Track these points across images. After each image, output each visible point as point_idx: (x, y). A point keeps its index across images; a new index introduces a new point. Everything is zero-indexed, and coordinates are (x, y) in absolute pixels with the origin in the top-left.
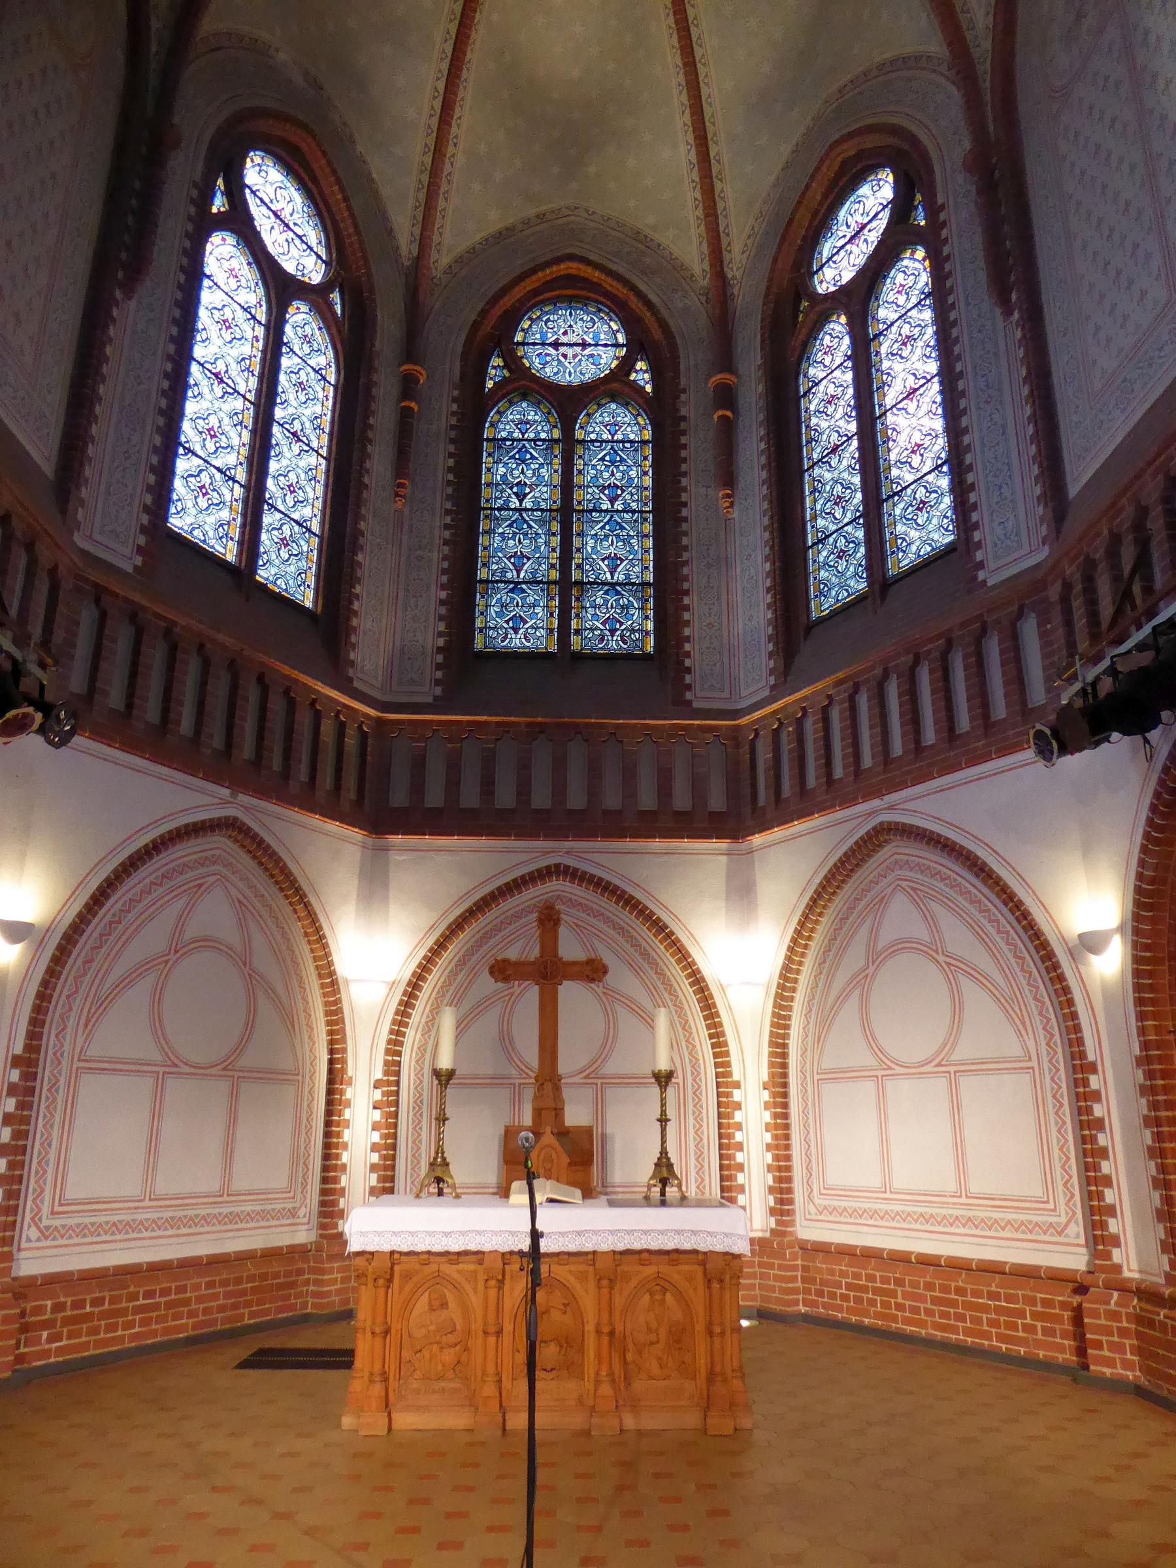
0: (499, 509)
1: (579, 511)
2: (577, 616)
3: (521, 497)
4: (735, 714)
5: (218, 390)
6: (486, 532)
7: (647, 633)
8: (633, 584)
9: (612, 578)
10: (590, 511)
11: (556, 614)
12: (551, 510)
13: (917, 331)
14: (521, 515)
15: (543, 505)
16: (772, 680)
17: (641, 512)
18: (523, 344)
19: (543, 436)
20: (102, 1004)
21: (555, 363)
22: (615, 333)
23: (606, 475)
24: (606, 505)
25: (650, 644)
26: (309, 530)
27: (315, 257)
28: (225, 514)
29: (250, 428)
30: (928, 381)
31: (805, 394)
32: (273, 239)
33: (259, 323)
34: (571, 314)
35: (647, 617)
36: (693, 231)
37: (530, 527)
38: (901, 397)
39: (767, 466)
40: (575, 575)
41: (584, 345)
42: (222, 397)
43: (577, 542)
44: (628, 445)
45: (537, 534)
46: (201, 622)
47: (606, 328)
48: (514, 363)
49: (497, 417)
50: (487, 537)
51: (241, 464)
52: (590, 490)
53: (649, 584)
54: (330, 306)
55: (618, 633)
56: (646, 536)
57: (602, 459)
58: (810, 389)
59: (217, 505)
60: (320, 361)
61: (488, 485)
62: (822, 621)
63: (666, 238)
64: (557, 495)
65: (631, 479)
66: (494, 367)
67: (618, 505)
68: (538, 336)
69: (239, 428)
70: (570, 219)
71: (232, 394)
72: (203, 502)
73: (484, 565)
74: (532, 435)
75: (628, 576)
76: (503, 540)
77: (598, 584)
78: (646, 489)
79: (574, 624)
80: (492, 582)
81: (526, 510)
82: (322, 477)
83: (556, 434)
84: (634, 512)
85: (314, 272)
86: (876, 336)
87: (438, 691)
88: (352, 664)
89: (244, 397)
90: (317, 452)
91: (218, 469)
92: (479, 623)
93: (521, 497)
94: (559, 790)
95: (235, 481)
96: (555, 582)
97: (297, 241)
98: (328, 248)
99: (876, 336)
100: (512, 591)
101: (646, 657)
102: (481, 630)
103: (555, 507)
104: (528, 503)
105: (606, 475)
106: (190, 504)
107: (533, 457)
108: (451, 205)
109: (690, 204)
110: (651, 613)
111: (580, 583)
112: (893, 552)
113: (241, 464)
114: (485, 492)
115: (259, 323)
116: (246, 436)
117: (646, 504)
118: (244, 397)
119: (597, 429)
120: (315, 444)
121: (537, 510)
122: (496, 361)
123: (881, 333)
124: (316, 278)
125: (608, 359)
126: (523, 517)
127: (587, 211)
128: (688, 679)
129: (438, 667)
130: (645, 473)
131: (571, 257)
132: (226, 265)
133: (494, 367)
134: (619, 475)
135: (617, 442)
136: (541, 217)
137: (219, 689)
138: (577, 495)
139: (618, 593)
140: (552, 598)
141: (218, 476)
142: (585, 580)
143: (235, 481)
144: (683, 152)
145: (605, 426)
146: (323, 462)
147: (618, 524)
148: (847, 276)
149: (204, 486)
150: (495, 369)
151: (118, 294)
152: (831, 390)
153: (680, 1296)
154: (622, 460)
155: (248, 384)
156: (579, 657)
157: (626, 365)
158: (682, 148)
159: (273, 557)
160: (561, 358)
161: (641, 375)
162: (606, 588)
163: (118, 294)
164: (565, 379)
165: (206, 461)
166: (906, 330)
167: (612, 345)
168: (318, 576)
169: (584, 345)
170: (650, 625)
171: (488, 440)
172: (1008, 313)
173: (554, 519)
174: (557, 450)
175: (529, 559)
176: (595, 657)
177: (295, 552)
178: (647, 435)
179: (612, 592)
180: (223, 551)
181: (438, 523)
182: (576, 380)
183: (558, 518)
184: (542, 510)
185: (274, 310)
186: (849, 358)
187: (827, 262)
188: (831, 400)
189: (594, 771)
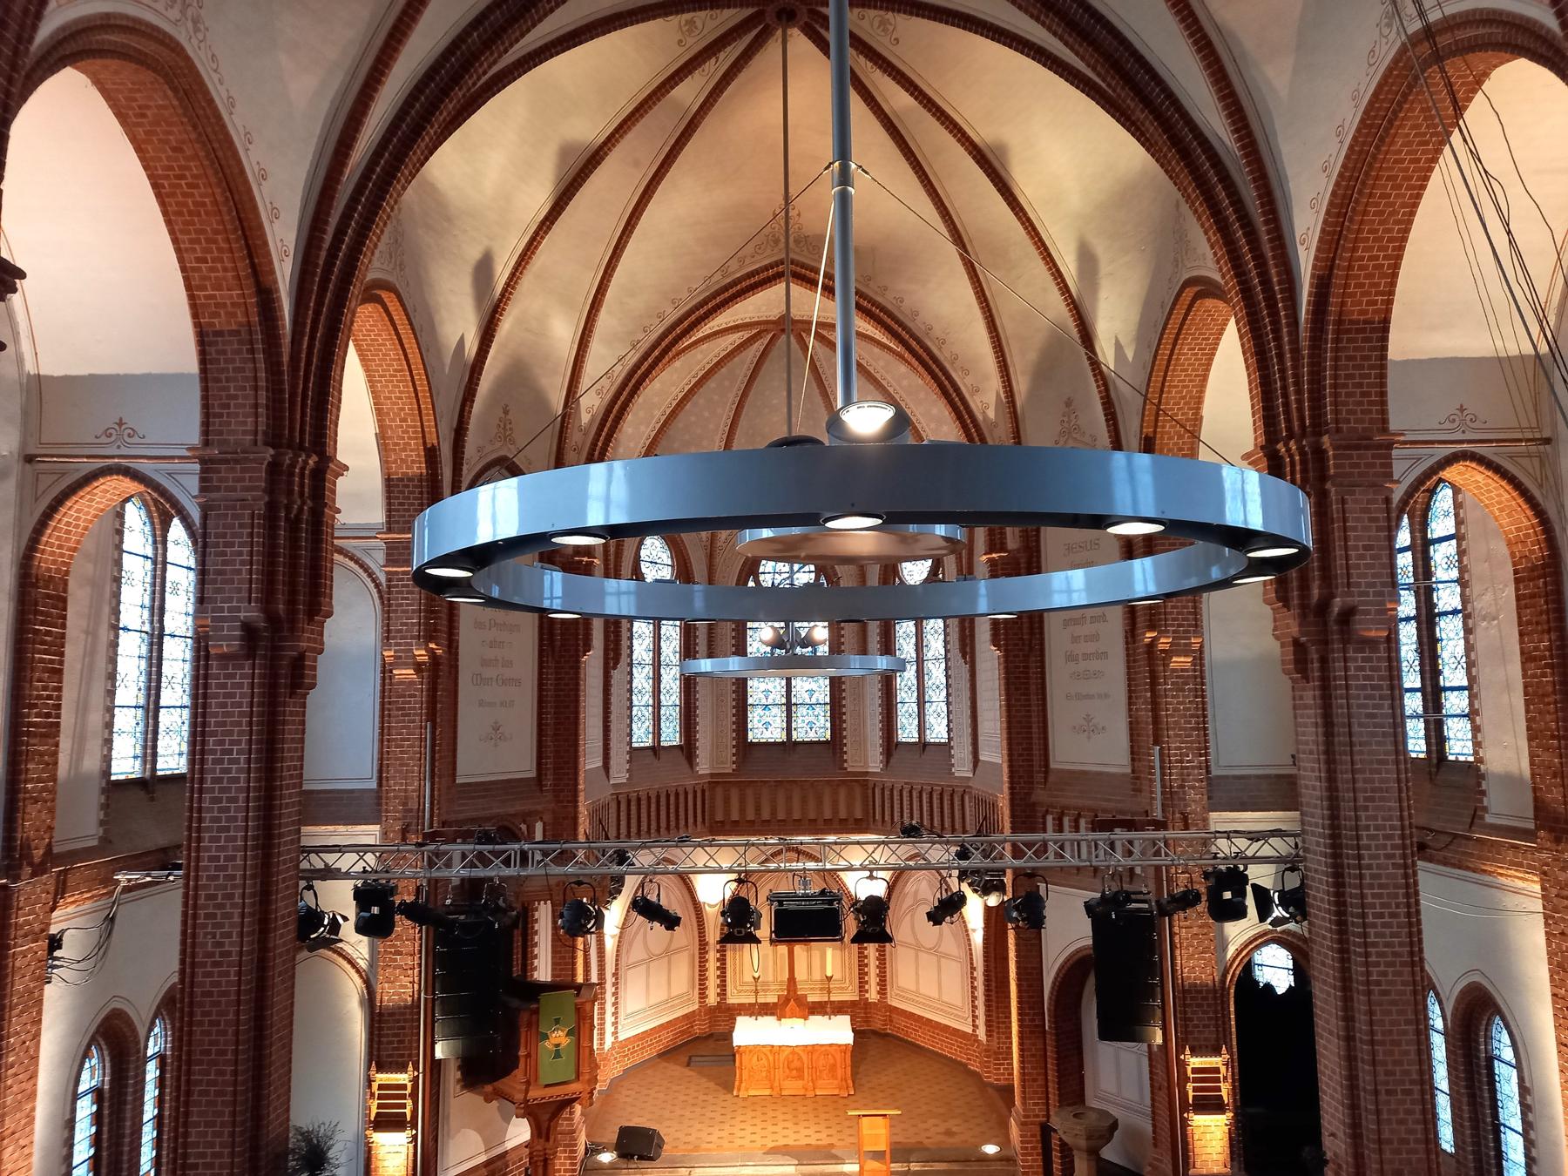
4: (867, 773)
20: (631, 945)
25: (828, 736)
28: (647, 723)
40: (794, 701)
79: (794, 725)
92: (750, 726)
94: (789, 811)
101: (827, 742)
137: (653, 807)
156: (796, 743)
170: (828, 725)
176: (804, 743)
189: (804, 801)
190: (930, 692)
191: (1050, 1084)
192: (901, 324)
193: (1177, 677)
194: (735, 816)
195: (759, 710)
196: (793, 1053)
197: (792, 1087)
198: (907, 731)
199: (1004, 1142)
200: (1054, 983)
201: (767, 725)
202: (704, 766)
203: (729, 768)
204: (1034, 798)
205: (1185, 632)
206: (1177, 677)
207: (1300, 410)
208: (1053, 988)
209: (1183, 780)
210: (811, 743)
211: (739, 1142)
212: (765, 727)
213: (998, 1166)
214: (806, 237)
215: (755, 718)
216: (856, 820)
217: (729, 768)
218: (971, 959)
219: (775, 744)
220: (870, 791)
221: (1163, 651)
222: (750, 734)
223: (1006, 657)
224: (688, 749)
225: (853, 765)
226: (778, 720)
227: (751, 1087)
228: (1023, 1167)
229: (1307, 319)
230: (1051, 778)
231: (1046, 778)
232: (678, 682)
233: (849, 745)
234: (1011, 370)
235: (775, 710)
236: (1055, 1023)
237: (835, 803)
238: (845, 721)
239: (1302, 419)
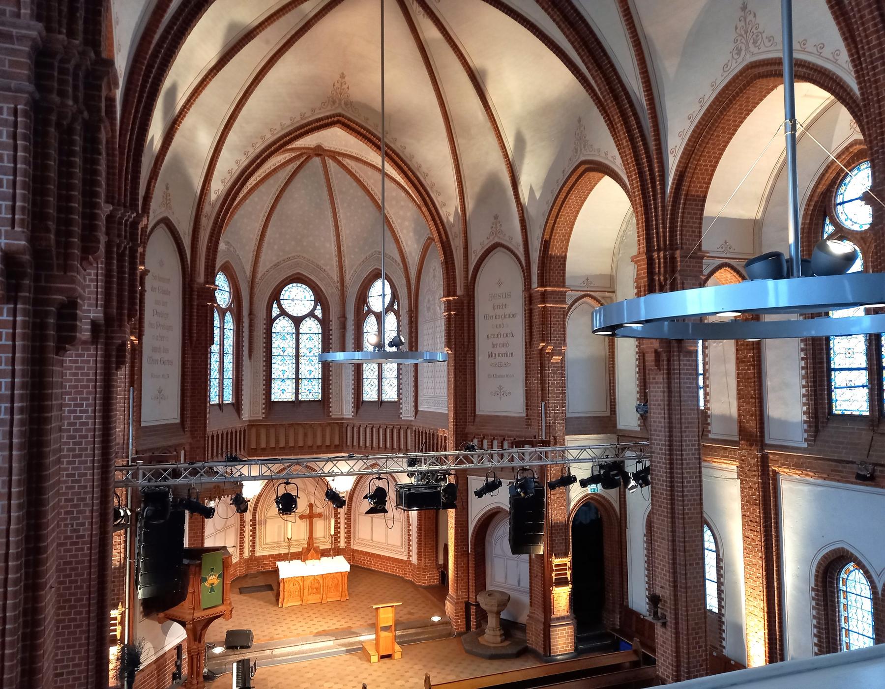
3: (284, 351)
24: (308, 354)
25: (320, 397)
40: (300, 377)
48: (280, 306)
63: (327, 268)
79: (300, 391)
83: (294, 331)
87: (264, 416)
93: (284, 351)
94: (296, 441)
101: (319, 401)
108: (263, 258)
109: (334, 260)
114: (273, 350)
122: (275, 305)
128: (331, 409)
129: (263, 409)
131: (298, 273)
144: (333, 247)
150: (275, 311)
153: (337, 579)
156: (301, 402)
157: (315, 308)
158: (333, 246)
161: (318, 313)
164: (295, 315)
170: (320, 391)
174: (294, 335)
176: (305, 401)
178: (320, 331)
182: (300, 315)
189: (305, 435)
190: (386, 372)
191: (470, 581)
192: (402, 160)
193: (554, 367)
194: (263, 445)
195: (279, 382)
196: (315, 579)
197: (313, 599)
198: (370, 394)
199: (443, 613)
200: (475, 528)
201: (283, 391)
202: (246, 416)
203: (260, 416)
204: (467, 430)
205: (559, 343)
206: (554, 367)
207: (664, 236)
208: (474, 530)
209: (555, 420)
210: (310, 401)
211: (296, 632)
212: (282, 392)
213: (441, 627)
214: (351, 103)
215: (276, 386)
216: (309, 447)
217: (260, 416)
218: (409, 520)
219: (288, 402)
220: (344, 429)
221: (548, 353)
222: (273, 396)
223: (455, 354)
224: (237, 405)
225: (334, 415)
226: (290, 388)
227: (289, 601)
228: (456, 626)
229: (671, 192)
230: (477, 420)
231: (474, 419)
232: (231, 364)
233: (333, 403)
234: (465, 195)
235: (288, 382)
236: (475, 549)
237: (323, 436)
239: (665, 241)
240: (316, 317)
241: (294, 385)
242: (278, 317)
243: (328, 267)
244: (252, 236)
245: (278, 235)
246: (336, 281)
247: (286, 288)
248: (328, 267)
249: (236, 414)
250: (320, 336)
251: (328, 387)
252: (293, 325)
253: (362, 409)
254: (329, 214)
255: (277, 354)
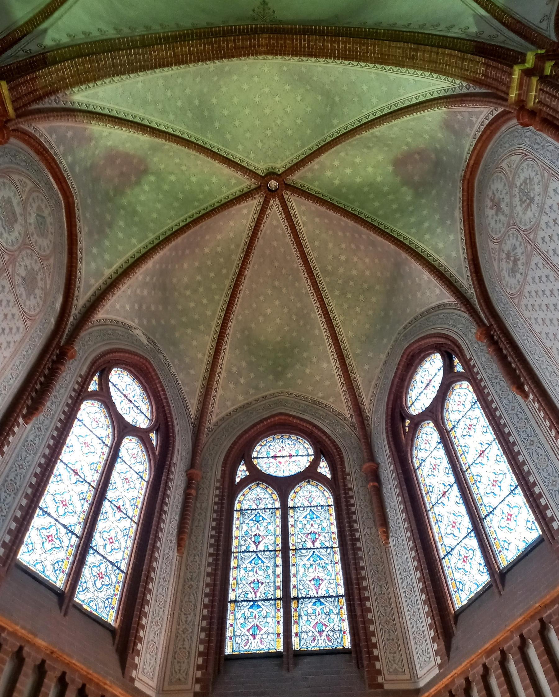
0: (243, 552)
1: (293, 550)
2: (296, 622)
3: (257, 543)
5: (74, 478)
6: (235, 568)
7: (344, 633)
8: (332, 597)
9: (317, 593)
10: (300, 549)
11: (281, 622)
12: (276, 551)
13: (475, 420)
14: (257, 555)
15: (271, 548)
16: (439, 660)
17: (332, 548)
18: (257, 458)
19: (270, 506)
21: (275, 466)
22: (307, 449)
23: (308, 526)
24: (309, 545)
25: (348, 644)
26: (119, 569)
27: (144, 417)
28: (62, 555)
29: (90, 502)
30: (489, 445)
31: (418, 468)
32: (122, 407)
33: (107, 445)
34: (282, 442)
35: (343, 620)
36: (342, 397)
37: (263, 562)
38: (476, 457)
39: (406, 510)
40: (294, 593)
41: (291, 456)
42: (75, 483)
43: (293, 570)
44: (319, 508)
45: (267, 567)
46: (23, 628)
47: (302, 447)
48: (252, 467)
49: (242, 497)
50: (235, 571)
51: (80, 523)
52: (299, 536)
53: (342, 596)
54: (150, 440)
55: (324, 634)
56: (336, 563)
57: (305, 517)
58: (420, 465)
59: (57, 548)
60: (140, 468)
61: (237, 537)
62: (463, 609)
63: (330, 402)
64: (279, 541)
65: (323, 528)
66: (240, 471)
67: (317, 545)
68: (265, 453)
69: (82, 501)
70: (279, 397)
71: (82, 482)
72: (48, 546)
73: (234, 590)
74: (263, 507)
75: (327, 591)
76: (246, 572)
77: (308, 598)
78: (333, 533)
79: (294, 629)
80: (238, 601)
81: (260, 551)
82: (132, 534)
83: (277, 504)
84: (327, 548)
85: (143, 423)
86: (451, 429)
88: (135, 667)
89: (90, 484)
90: (131, 519)
91: (64, 526)
92: (229, 632)
93: (257, 543)
95: (73, 533)
96: (279, 599)
97: (135, 409)
98: (152, 413)
99: (451, 429)
100: (252, 607)
102: (230, 638)
103: (278, 548)
104: (261, 547)
105: (308, 526)
106: (38, 546)
107: (264, 519)
109: (339, 385)
110: (345, 617)
111: (297, 598)
112: (500, 551)
113: (80, 523)
114: (235, 542)
115: (107, 445)
116: (86, 507)
117: (334, 543)
118: (90, 484)
119: (301, 500)
120: (130, 515)
121: (267, 551)
123: (454, 427)
124: (144, 426)
125: (303, 463)
126: (258, 557)
127: (288, 393)
129: (199, 668)
130: (332, 524)
131: (281, 414)
132: (92, 416)
133: (240, 471)
134: (316, 526)
135: (313, 506)
136: (265, 398)
138: (292, 540)
139: (322, 604)
140: (278, 610)
141: (63, 530)
142: (300, 596)
143: (73, 533)
145: (306, 498)
146: (135, 526)
147: (318, 556)
148: (428, 403)
149: (51, 536)
151: (21, 420)
152: (433, 462)
154: (317, 517)
155: (94, 477)
157: (314, 464)
158: (332, 362)
159: (90, 585)
160: (278, 464)
161: (324, 469)
162: (314, 600)
163: (21, 420)
164: (280, 474)
165: (56, 520)
166: (468, 422)
167: (306, 455)
168: (120, 601)
169: (291, 456)
170: (346, 626)
171: (237, 511)
172: (526, 396)
173: (278, 556)
174: (278, 513)
175: (262, 583)
177: (107, 583)
178: (331, 501)
179: (318, 604)
180: (55, 579)
181: (203, 562)
182: (287, 474)
183: (281, 555)
184: (271, 551)
185: (116, 439)
186: (439, 443)
187: (416, 400)
188: (435, 467)
195: (245, 610)
232: (130, 543)
235: (266, 609)
238: (369, 610)
240: (321, 479)
241: (281, 614)
242: (245, 482)
243: (331, 400)
244: (200, 356)
245: (244, 364)
246: (348, 416)
247: (263, 442)
248: (331, 400)
249: (113, 659)
250: (332, 510)
251: (362, 605)
252: (275, 496)
253: (459, 633)
254: (317, 315)
255: (243, 548)
